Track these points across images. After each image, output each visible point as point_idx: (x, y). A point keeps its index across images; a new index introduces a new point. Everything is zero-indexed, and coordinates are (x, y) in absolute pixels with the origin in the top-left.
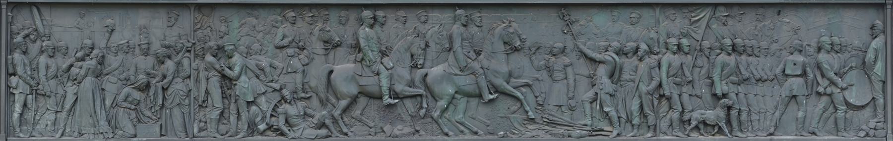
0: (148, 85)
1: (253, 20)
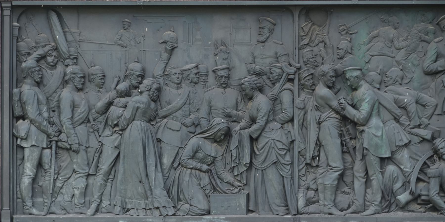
0: (228, 134)
1: (391, 32)
